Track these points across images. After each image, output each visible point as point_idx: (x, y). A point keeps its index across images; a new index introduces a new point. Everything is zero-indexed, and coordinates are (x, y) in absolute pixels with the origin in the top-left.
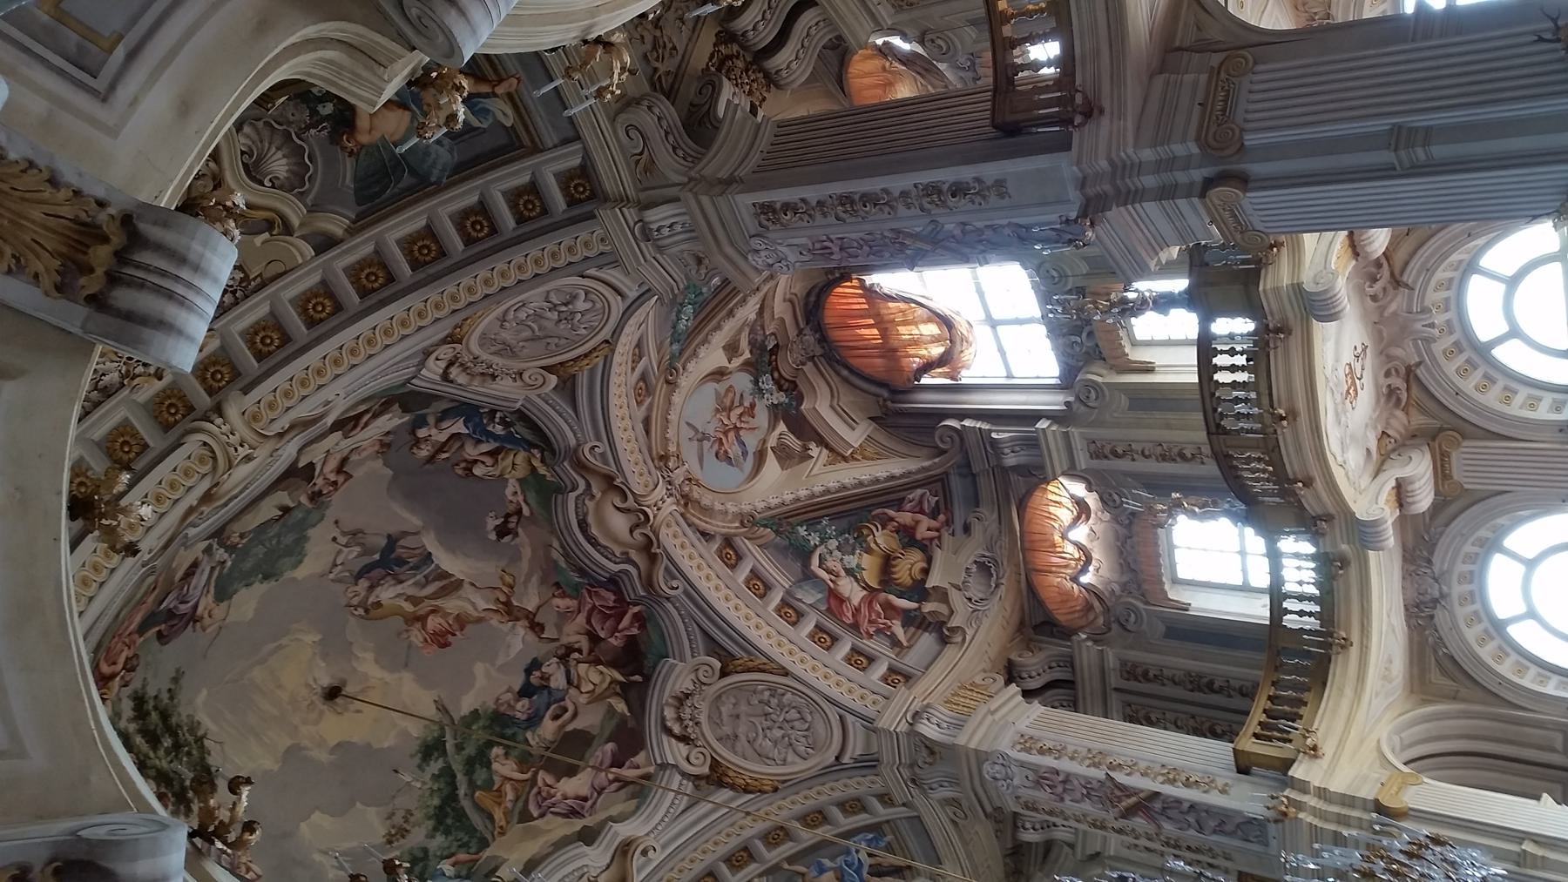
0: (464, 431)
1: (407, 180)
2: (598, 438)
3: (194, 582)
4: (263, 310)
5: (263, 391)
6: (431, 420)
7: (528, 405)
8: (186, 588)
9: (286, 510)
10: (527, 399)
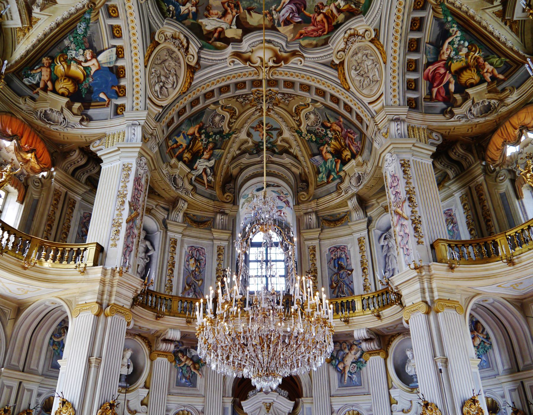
0: (181, 7)
1: (192, 119)
2: (141, 4)
3: (287, 15)
4: (237, 92)
5: (250, 78)
6: (191, 14)
7: (162, 21)
8: (290, 16)
9: (249, 10)
10: (163, 25)
